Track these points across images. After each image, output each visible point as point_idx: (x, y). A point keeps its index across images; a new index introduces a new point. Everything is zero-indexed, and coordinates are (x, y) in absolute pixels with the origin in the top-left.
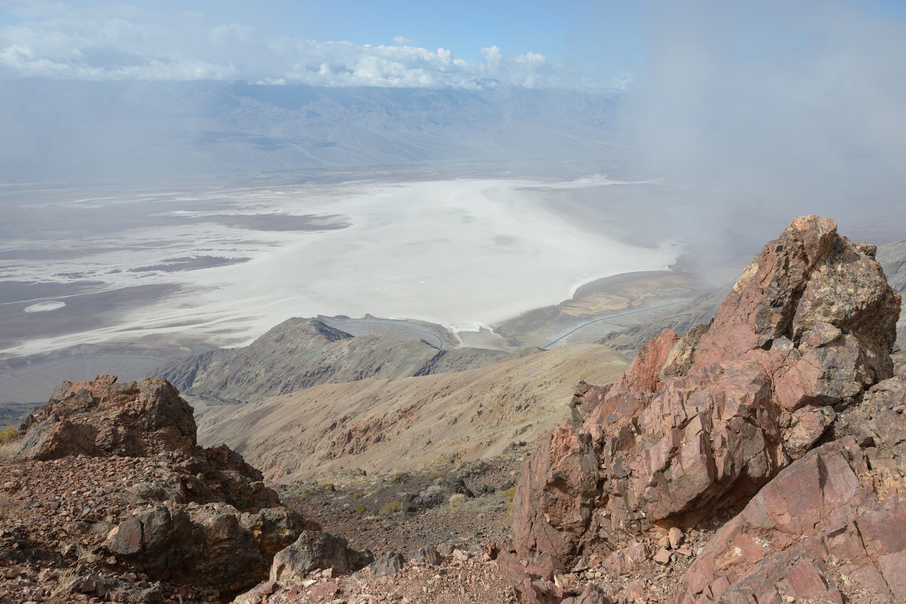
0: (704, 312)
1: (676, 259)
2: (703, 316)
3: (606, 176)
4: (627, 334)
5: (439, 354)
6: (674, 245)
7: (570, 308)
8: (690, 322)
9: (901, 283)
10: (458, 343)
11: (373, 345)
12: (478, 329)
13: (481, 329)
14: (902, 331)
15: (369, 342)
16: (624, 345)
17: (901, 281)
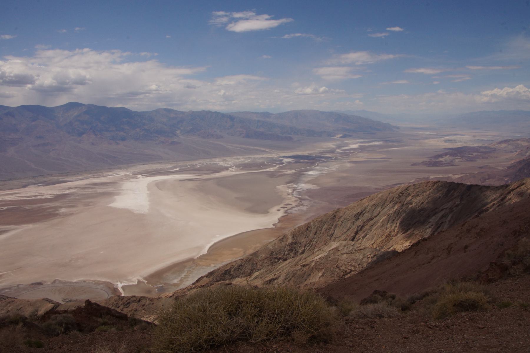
0: (251, 257)
1: (278, 219)
2: (250, 259)
3: (241, 168)
4: (207, 277)
5: (53, 307)
6: (279, 210)
7: (204, 260)
8: (243, 264)
9: (360, 225)
10: (121, 294)
11: (10, 306)
12: (137, 282)
13: (139, 282)
14: (324, 259)
15: (7, 304)
16: (202, 285)
17: (360, 224)
